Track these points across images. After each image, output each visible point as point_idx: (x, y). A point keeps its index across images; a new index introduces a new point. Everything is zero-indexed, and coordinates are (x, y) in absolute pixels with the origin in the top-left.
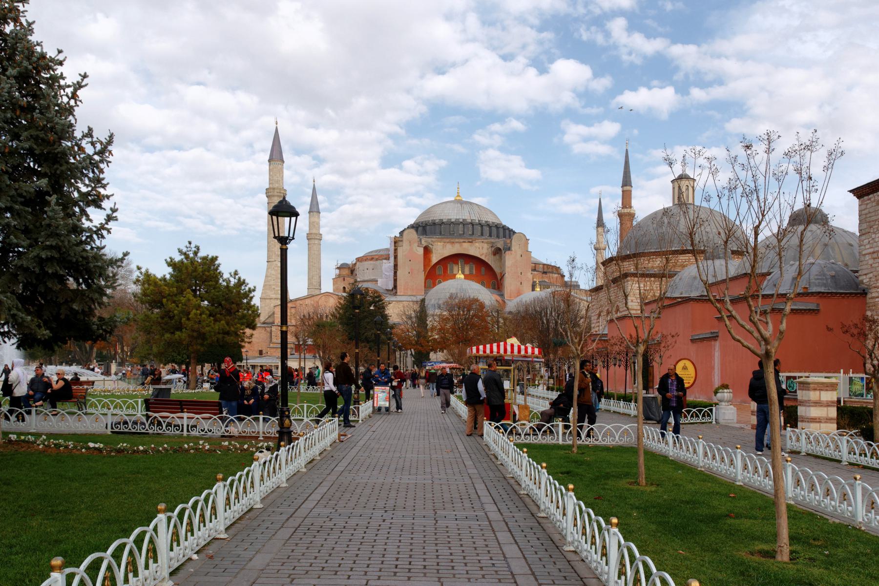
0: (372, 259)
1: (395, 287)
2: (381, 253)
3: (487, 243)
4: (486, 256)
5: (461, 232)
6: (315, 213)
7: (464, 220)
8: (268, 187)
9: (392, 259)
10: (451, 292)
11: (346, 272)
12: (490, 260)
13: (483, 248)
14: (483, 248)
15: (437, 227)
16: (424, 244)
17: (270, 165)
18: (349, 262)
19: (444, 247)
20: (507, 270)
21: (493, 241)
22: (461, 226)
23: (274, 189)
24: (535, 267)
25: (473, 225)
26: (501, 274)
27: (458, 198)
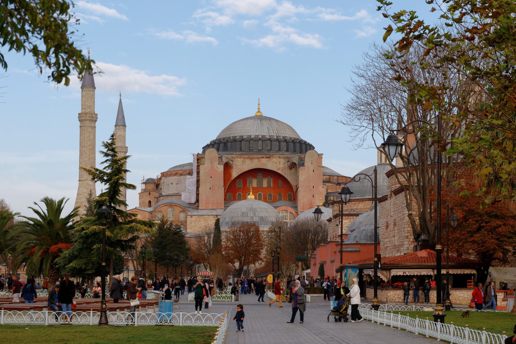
0: (176, 174)
1: (197, 201)
2: (185, 168)
3: (284, 158)
4: (282, 170)
5: (260, 148)
6: (121, 127)
7: (263, 136)
8: (80, 112)
9: (195, 174)
10: (242, 211)
11: (152, 186)
12: (287, 174)
13: (279, 162)
14: (279, 162)
15: (238, 144)
16: (225, 160)
17: (82, 91)
18: (155, 177)
19: (243, 162)
20: (300, 185)
21: (289, 156)
22: (260, 142)
23: (86, 114)
24: (330, 178)
25: (271, 141)
26: (297, 186)
27: (258, 114)
